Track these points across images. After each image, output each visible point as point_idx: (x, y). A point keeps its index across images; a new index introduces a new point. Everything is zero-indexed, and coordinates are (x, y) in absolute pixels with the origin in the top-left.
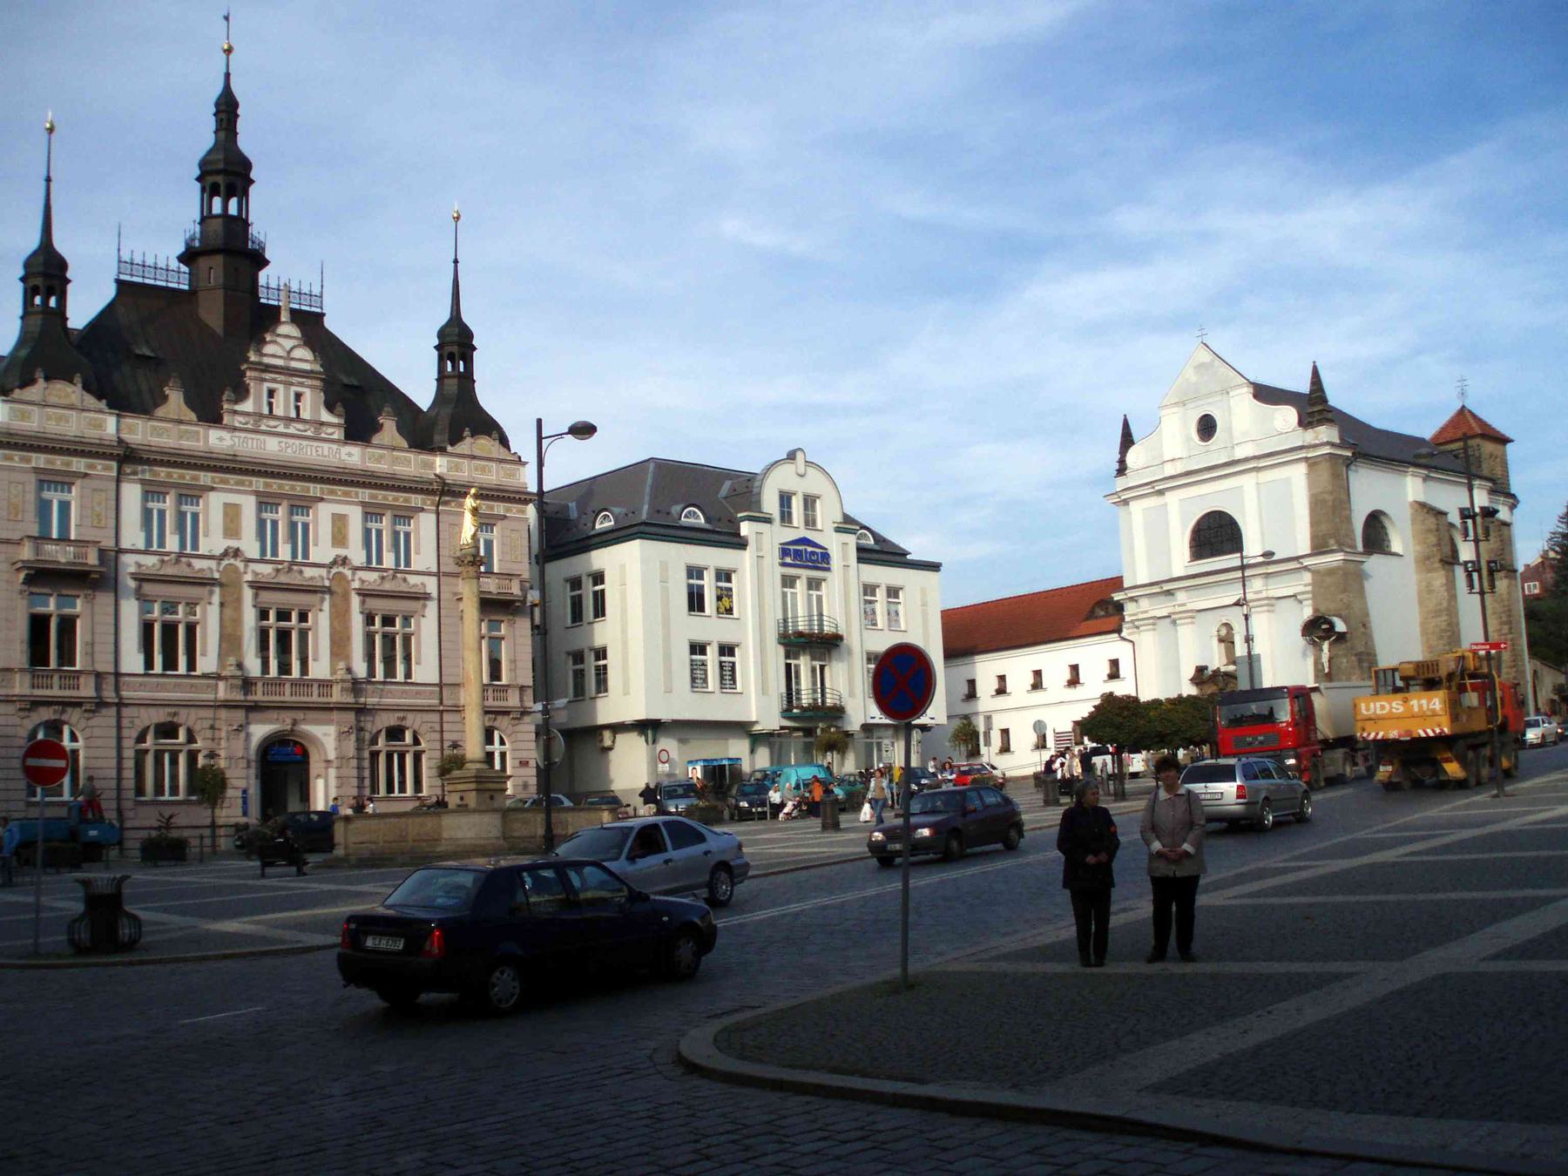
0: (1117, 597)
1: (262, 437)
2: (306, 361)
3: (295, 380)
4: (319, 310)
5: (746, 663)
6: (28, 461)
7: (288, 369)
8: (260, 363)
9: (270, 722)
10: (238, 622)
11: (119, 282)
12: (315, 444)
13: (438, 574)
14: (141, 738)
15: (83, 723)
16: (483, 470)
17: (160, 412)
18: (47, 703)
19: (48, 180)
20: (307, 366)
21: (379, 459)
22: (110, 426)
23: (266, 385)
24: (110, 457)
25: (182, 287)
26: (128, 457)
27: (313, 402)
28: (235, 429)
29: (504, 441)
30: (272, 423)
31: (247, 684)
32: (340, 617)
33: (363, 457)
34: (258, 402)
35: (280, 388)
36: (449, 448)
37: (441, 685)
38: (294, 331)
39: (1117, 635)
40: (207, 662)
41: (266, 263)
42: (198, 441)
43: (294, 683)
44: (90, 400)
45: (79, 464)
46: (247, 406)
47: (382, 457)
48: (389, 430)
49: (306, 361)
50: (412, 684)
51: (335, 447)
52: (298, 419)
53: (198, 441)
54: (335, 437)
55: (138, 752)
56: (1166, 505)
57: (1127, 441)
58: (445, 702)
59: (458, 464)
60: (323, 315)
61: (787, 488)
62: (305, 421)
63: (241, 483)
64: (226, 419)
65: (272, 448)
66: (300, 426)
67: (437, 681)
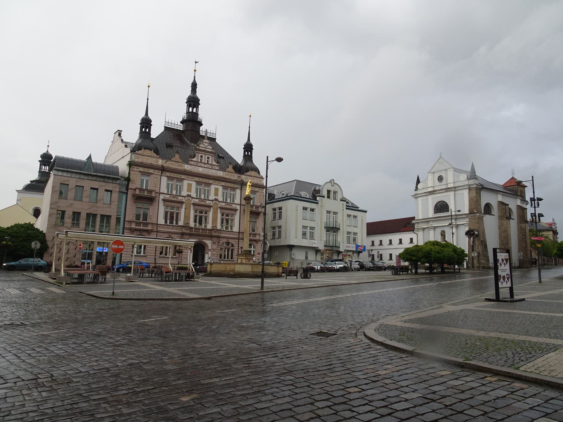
0: (413, 222)
1: (198, 167)
3: (207, 154)
5: (317, 233)
6: (138, 169)
7: (206, 151)
10: (190, 213)
11: (165, 127)
12: (211, 170)
13: (240, 205)
17: (173, 159)
20: (210, 151)
21: (227, 175)
22: (160, 162)
23: (200, 155)
24: (159, 169)
25: (181, 129)
26: (163, 169)
27: (212, 161)
28: (192, 165)
29: (259, 173)
30: (201, 164)
32: (215, 214)
33: (223, 174)
34: (198, 158)
35: (204, 155)
36: (245, 173)
37: (239, 232)
40: (181, 223)
41: (202, 125)
42: (182, 167)
43: (203, 229)
44: (155, 155)
45: (151, 171)
46: (195, 159)
50: (233, 232)
51: (216, 171)
52: (208, 163)
53: (182, 167)
54: (217, 168)
56: (428, 199)
57: (418, 182)
59: (247, 177)
61: (329, 189)
62: (209, 164)
63: (193, 179)
64: (190, 162)
65: (200, 170)
66: (208, 165)
67: (238, 231)
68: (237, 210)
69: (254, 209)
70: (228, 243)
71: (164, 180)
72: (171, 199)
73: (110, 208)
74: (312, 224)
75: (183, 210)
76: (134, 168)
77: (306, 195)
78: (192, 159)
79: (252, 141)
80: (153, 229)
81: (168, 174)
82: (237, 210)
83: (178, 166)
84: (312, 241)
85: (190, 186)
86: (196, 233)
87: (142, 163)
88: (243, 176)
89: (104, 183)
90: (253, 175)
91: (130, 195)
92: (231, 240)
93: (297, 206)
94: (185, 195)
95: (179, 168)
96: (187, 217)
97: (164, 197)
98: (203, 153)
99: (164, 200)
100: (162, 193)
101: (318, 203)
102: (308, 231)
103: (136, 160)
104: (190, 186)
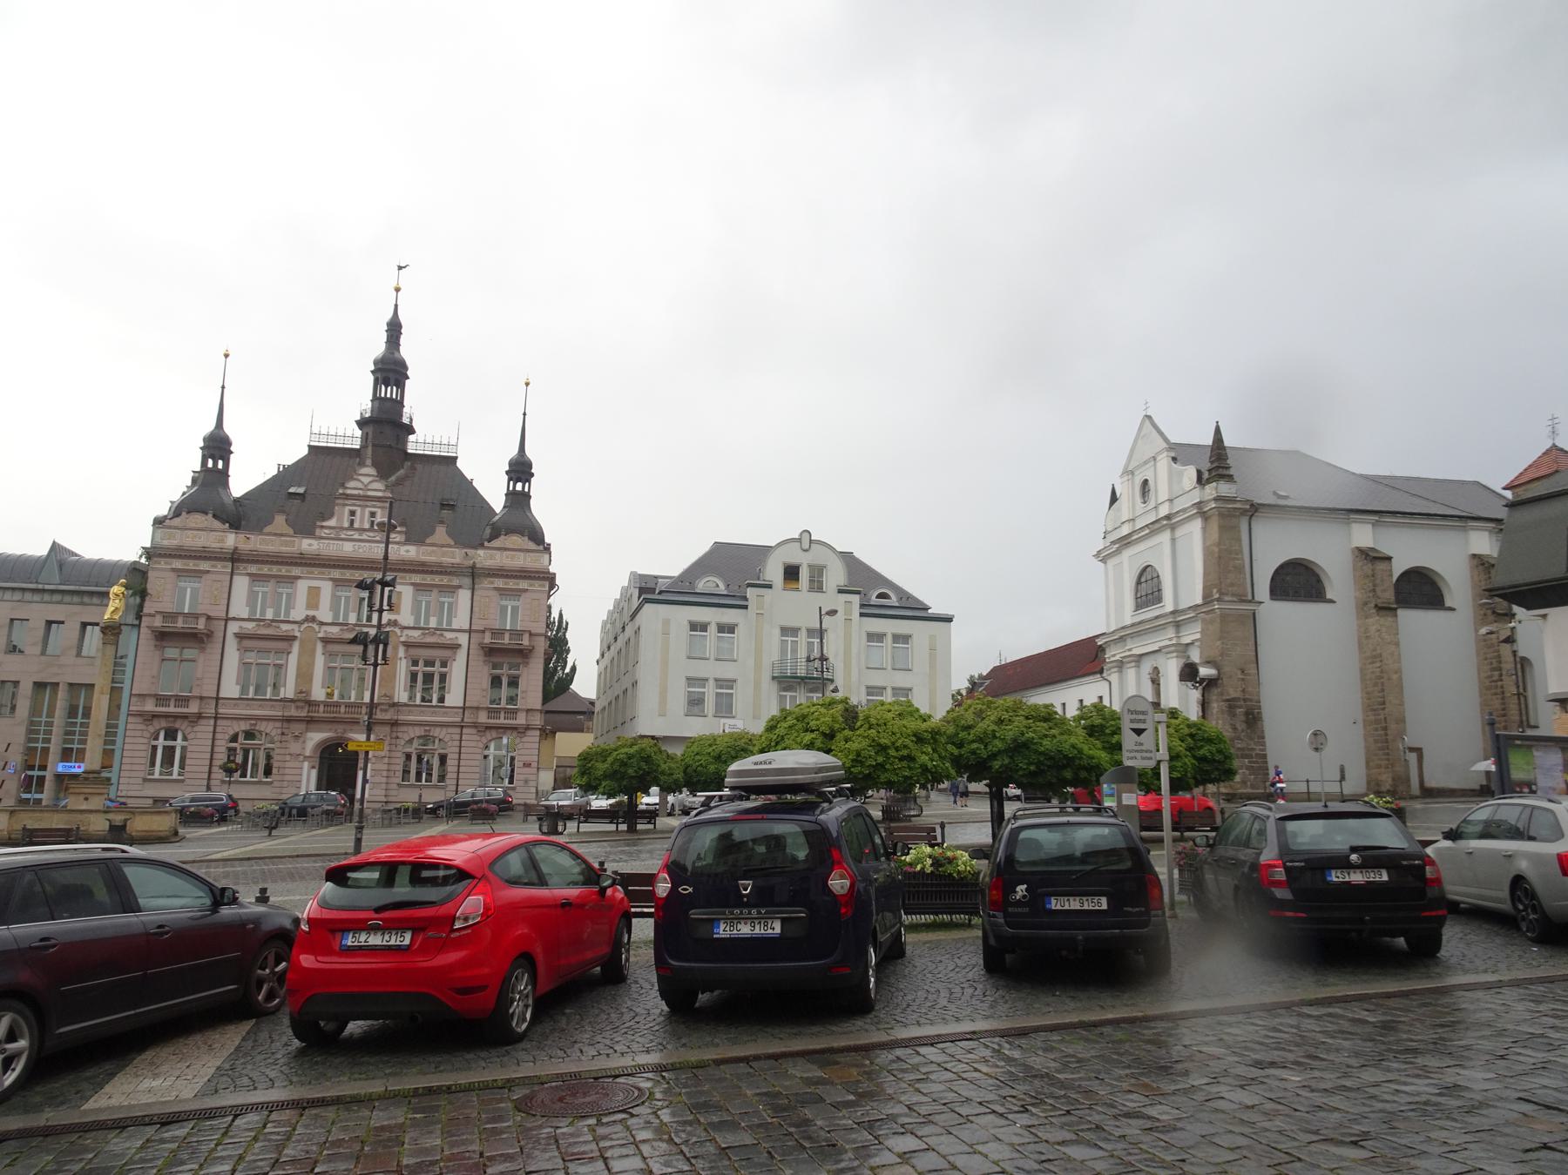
1: (340, 542)
2: (380, 490)
3: (369, 503)
4: (454, 455)
5: (742, 697)
8: (344, 494)
9: (330, 730)
10: (311, 665)
11: (310, 446)
13: (470, 631)
14: (234, 739)
15: (189, 729)
16: (513, 558)
17: (268, 529)
18: (166, 716)
19: (223, 387)
20: (380, 494)
21: (430, 554)
22: (231, 540)
24: (224, 559)
25: (354, 447)
31: (311, 704)
36: (486, 544)
37: (464, 708)
38: (372, 471)
39: (1099, 676)
44: (217, 524)
46: (332, 522)
47: (433, 551)
48: (441, 534)
49: (380, 490)
50: (444, 707)
54: (397, 540)
55: (230, 749)
58: (465, 720)
60: (456, 458)
61: (793, 561)
63: (323, 573)
64: (318, 532)
65: (348, 549)
67: (462, 705)
68: (458, 646)
69: (507, 641)
70: (426, 739)
71: (241, 584)
72: (258, 632)
73: (93, 665)
74: (727, 671)
75: (293, 659)
76: (160, 563)
77: (718, 586)
78: (324, 524)
79: (530, 453)
80: (202, 711)
81: (253, 569)
82: (458, 646)
83: (286, 544)
84: (723, 721)
85: (314, 593)
86: (328, 715)
87: (180, 548)
88: (481, 552)
89: (80, 607)
90: (511, 546)
91: (143, 630)
92: (438, 729)
93: (666, 623)
94: (299, 618)
95: (284, 549)
96: (305, 675)
97: (241, 627)
98: (358, 503)
99: (241, 637)
100: (234, 619)
101: (746, 607)
102: (710, 692)
103: (166, 543)
104: (314, 593)
